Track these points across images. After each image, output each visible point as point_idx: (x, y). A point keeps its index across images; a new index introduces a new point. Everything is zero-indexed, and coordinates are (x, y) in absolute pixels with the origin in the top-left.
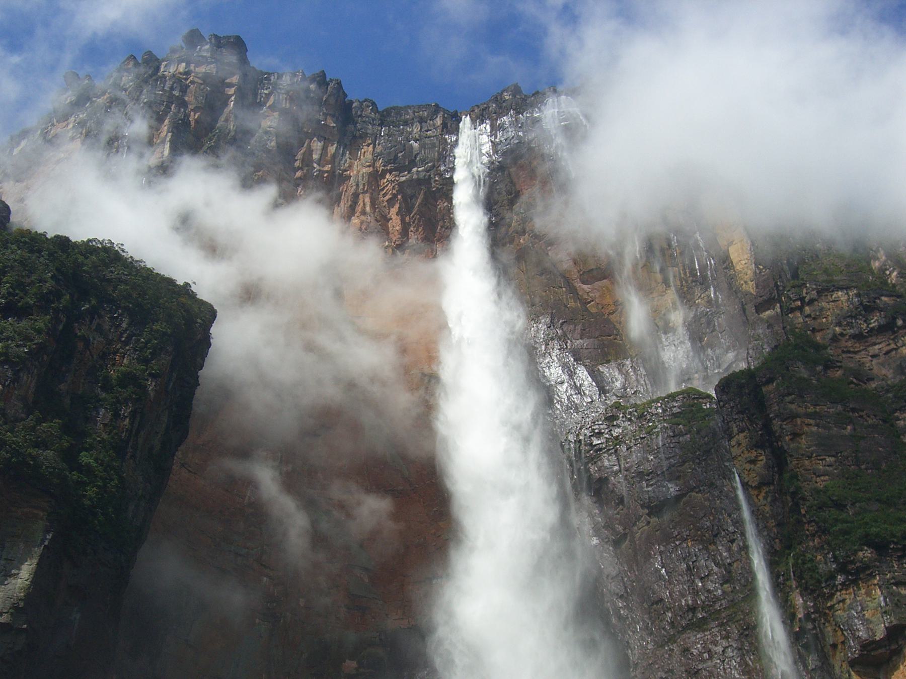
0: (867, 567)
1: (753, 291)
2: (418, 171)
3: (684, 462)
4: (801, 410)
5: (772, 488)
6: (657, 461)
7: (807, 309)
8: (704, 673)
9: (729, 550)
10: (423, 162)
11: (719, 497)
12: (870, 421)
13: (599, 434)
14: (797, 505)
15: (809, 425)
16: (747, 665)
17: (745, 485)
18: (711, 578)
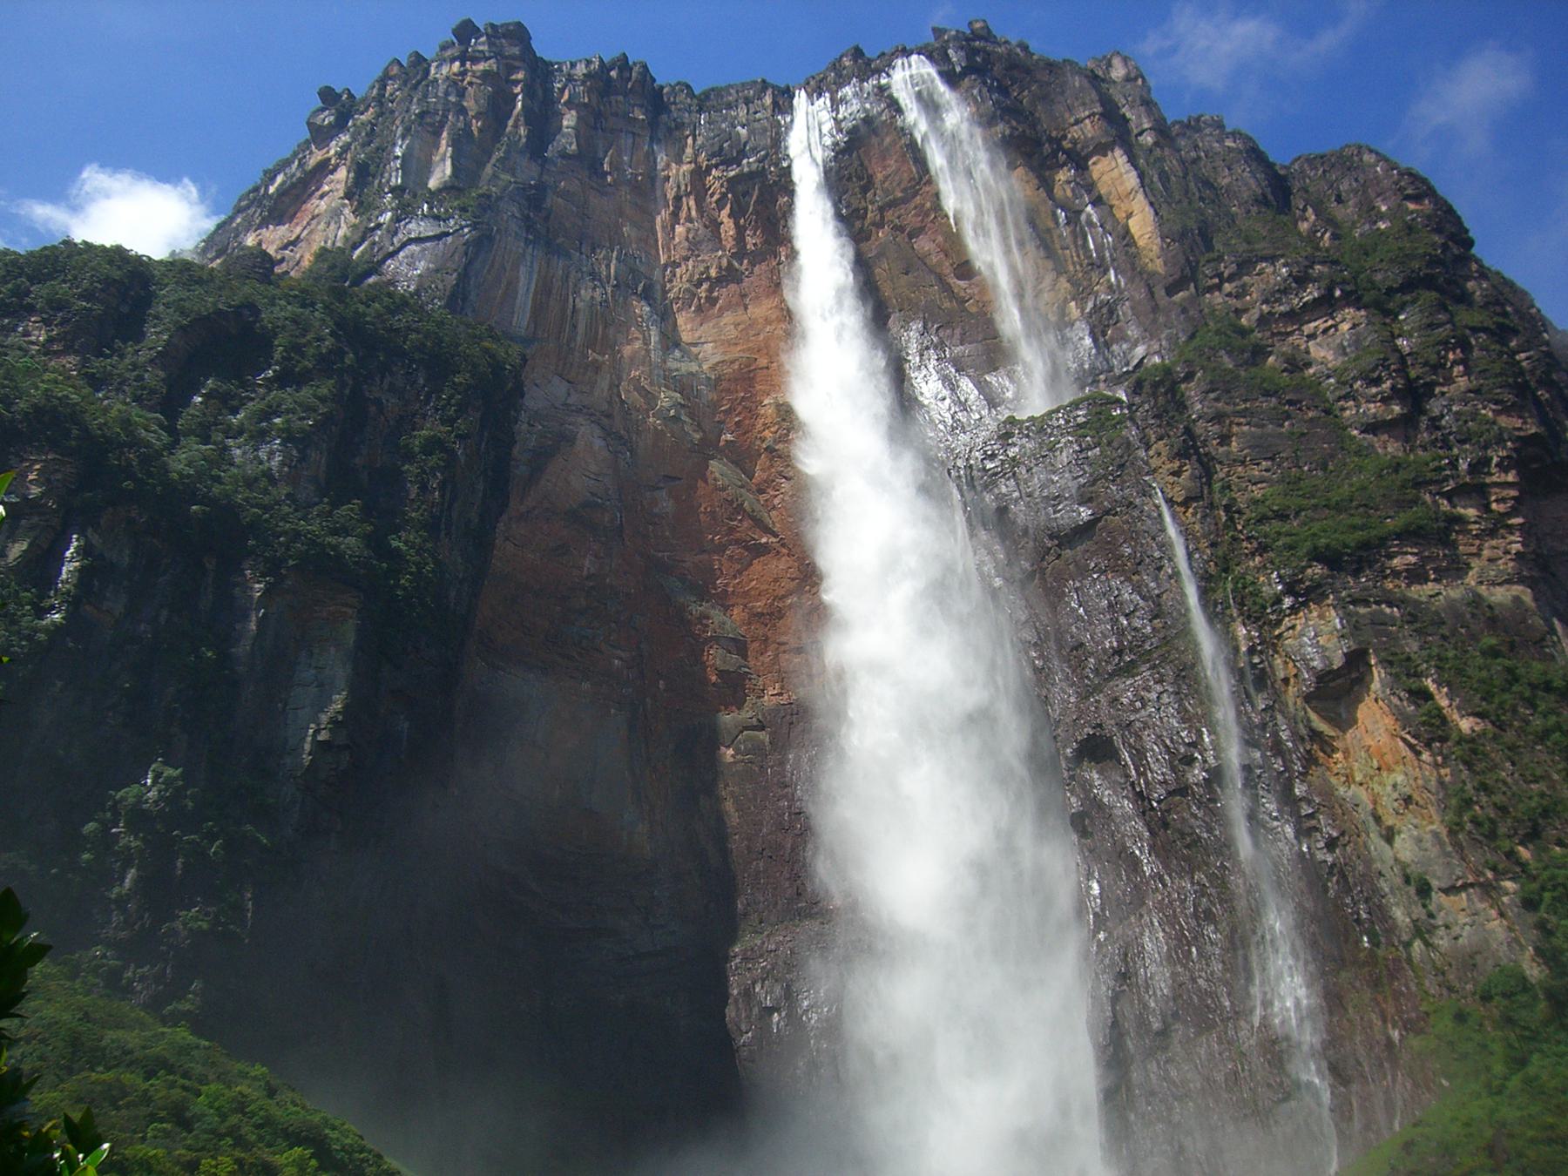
0: (1319, 586)
1: (1161, 270)
2: (748, 164)
3: (1094, 483)
4: (1229, 409)
6: (1063, 482)
7: (1227, 287)
8: (1138, 724)
9: (1156, 579)
10: (754, 150)
11: (1140, 520)
12: (1310, 414)
13: (993, 457)
14: (1231, 519)
15: (1239, 424)
16: (1187, 711)
17: (1170, 502)
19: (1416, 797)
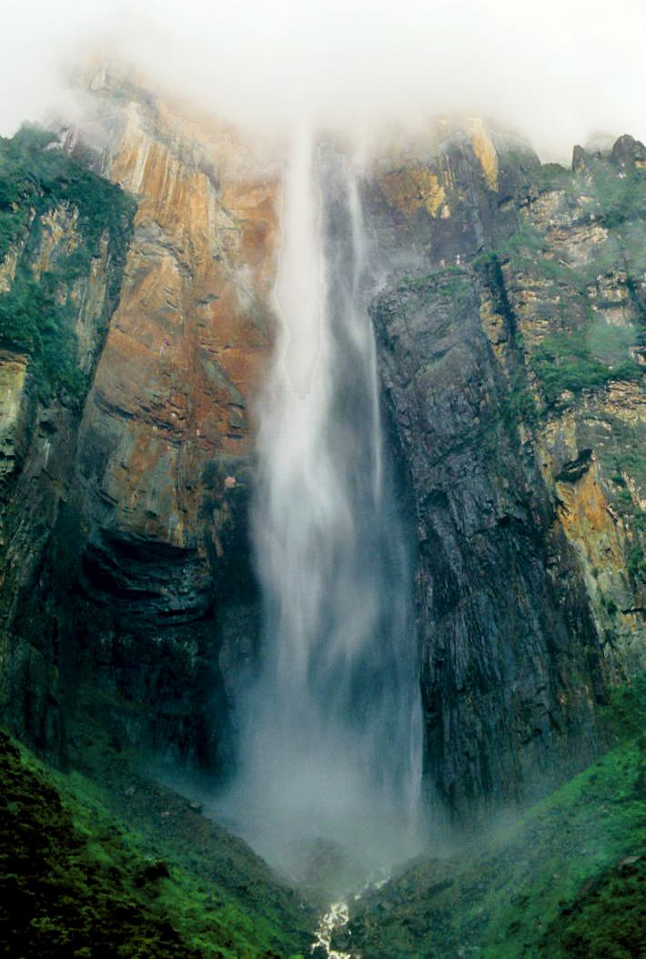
1: (497, 191)
4: (526, 285)
5: (506, 344)
8: (461, 487)
14: (523, 357)
15: (531, 296)
16: (489, 480)
18: (466, 413)
19: (613, 549)
